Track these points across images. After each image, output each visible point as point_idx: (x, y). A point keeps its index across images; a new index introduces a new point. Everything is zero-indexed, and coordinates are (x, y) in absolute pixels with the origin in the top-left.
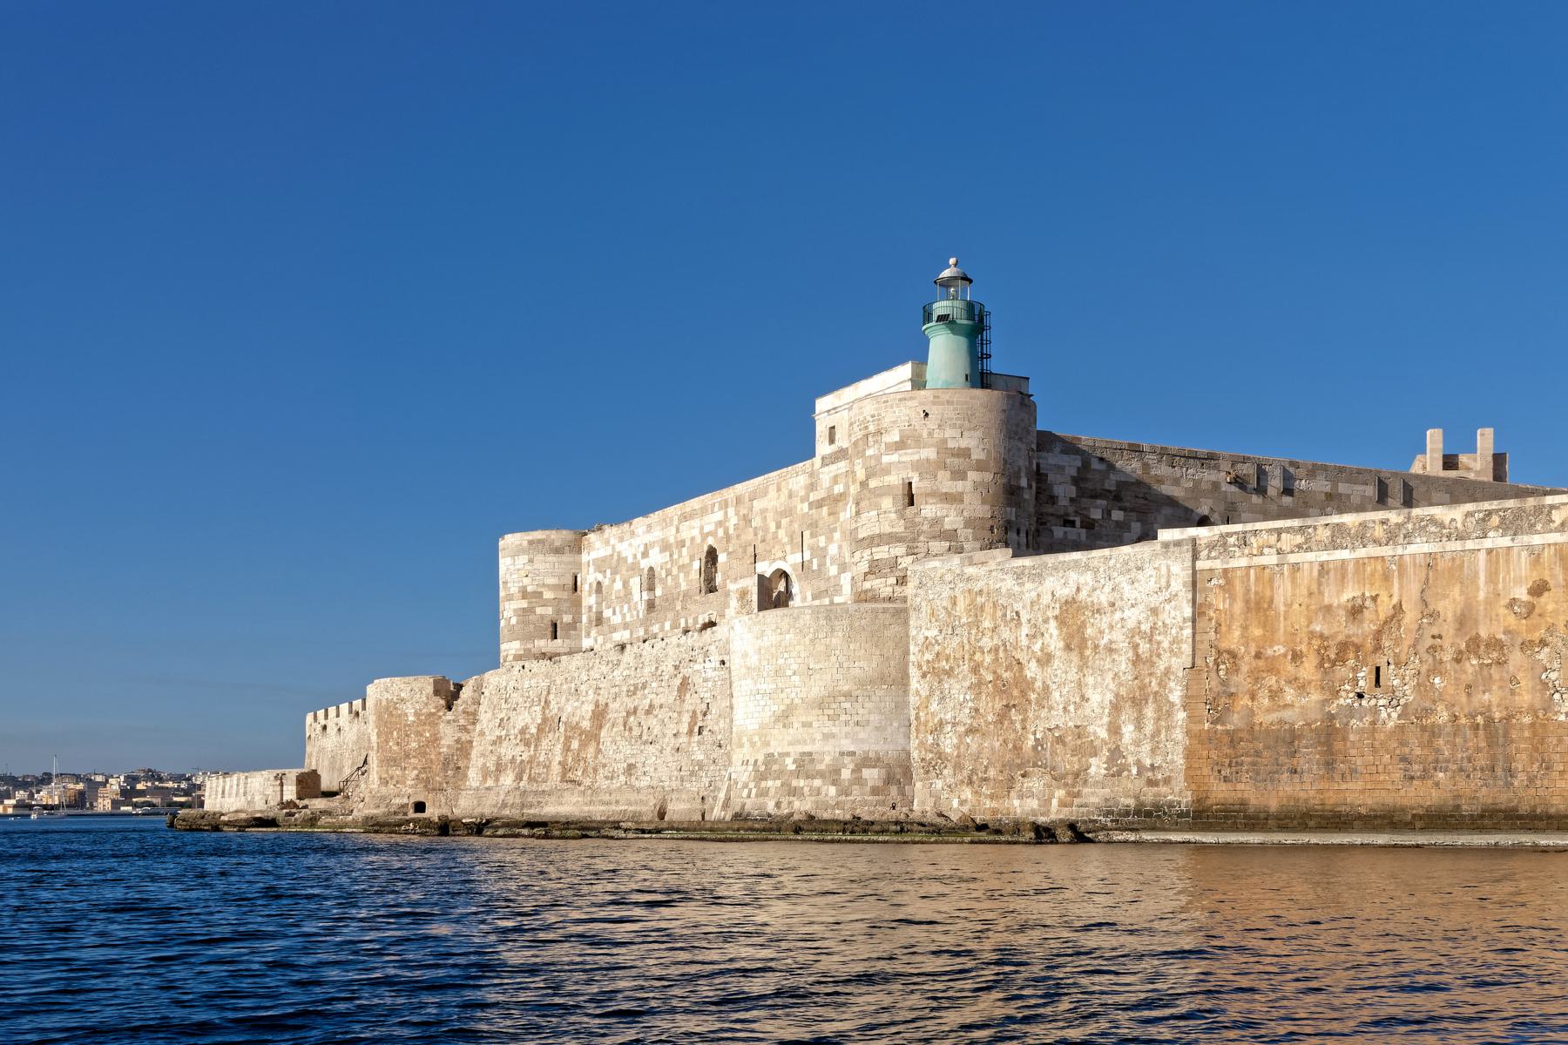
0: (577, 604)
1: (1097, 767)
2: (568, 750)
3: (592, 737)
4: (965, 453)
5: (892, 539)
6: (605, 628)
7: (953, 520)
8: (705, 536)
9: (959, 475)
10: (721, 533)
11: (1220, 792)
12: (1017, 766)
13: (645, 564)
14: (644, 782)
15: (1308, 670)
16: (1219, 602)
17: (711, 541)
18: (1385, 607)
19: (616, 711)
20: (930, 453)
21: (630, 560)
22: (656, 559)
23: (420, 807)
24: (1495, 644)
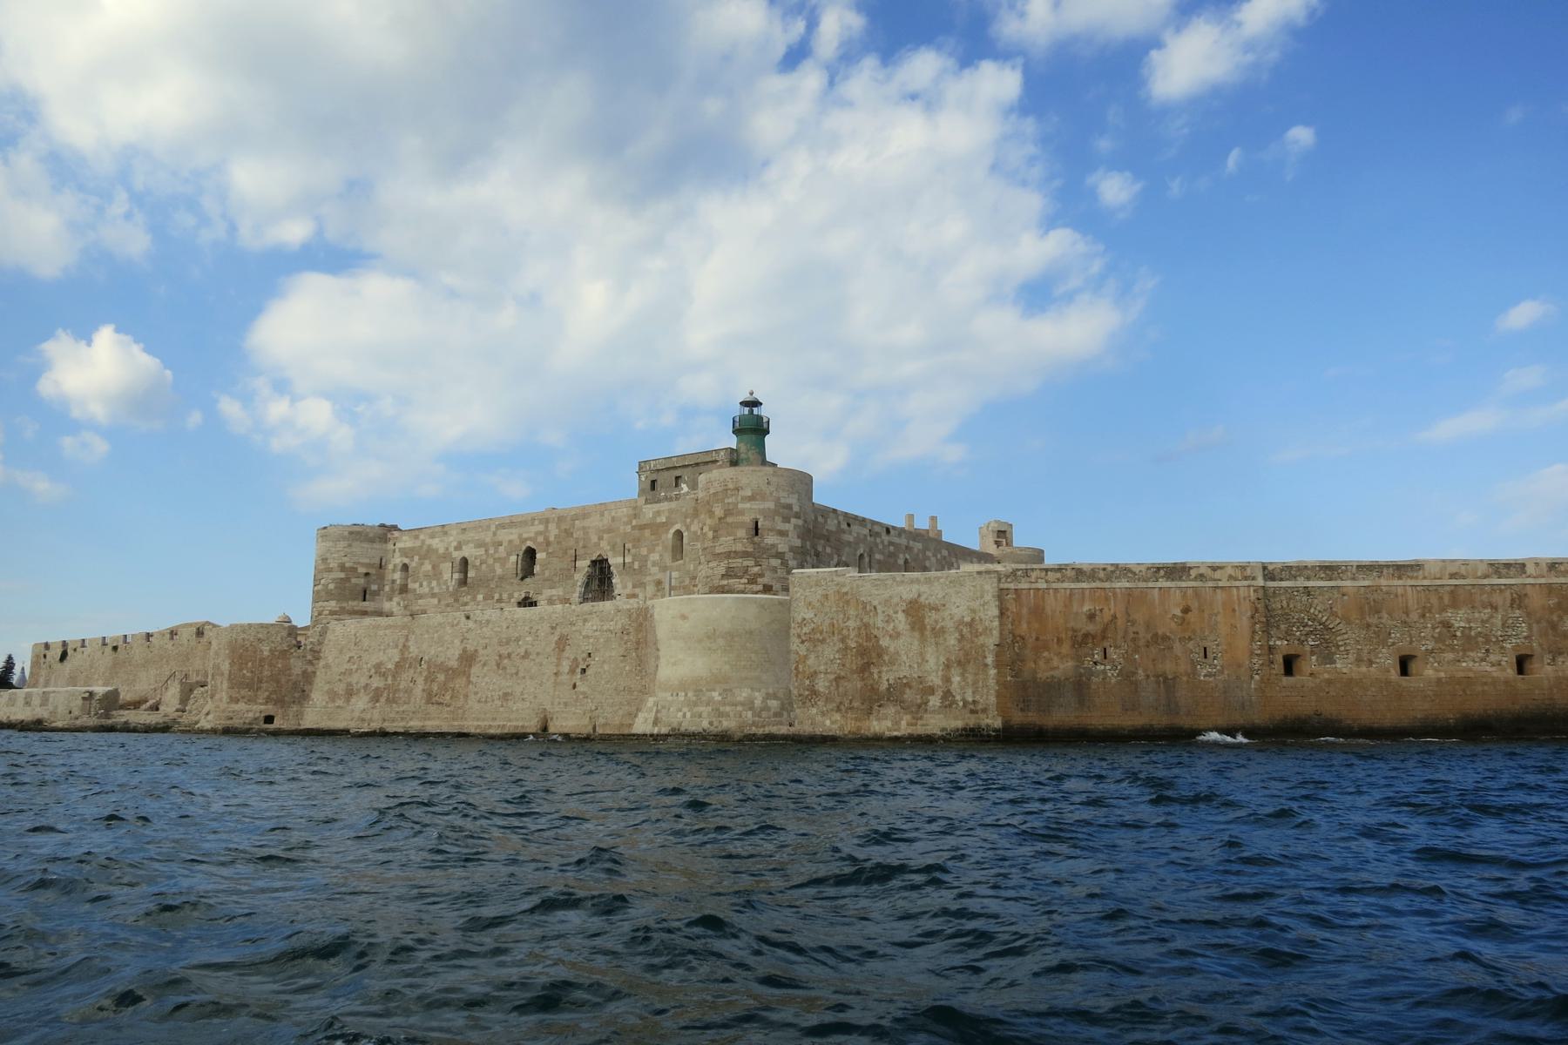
0: (381, 578)
1: (935, 701)
4: (789, 507)
5: (746, 555)
6: (410, 596)
7: (783, 547)
9: (786, 520)
11: (1018, 718)
12: (873, 699)
13: (457, 555)
15: (1066, 648)
16: (1013, 607)
17: (529, 544)
18: (1107, 616)
20: (771, 505)
21: (441, 551)
22: (467, 551)
23: (269, 719)
24: (1165, 638)
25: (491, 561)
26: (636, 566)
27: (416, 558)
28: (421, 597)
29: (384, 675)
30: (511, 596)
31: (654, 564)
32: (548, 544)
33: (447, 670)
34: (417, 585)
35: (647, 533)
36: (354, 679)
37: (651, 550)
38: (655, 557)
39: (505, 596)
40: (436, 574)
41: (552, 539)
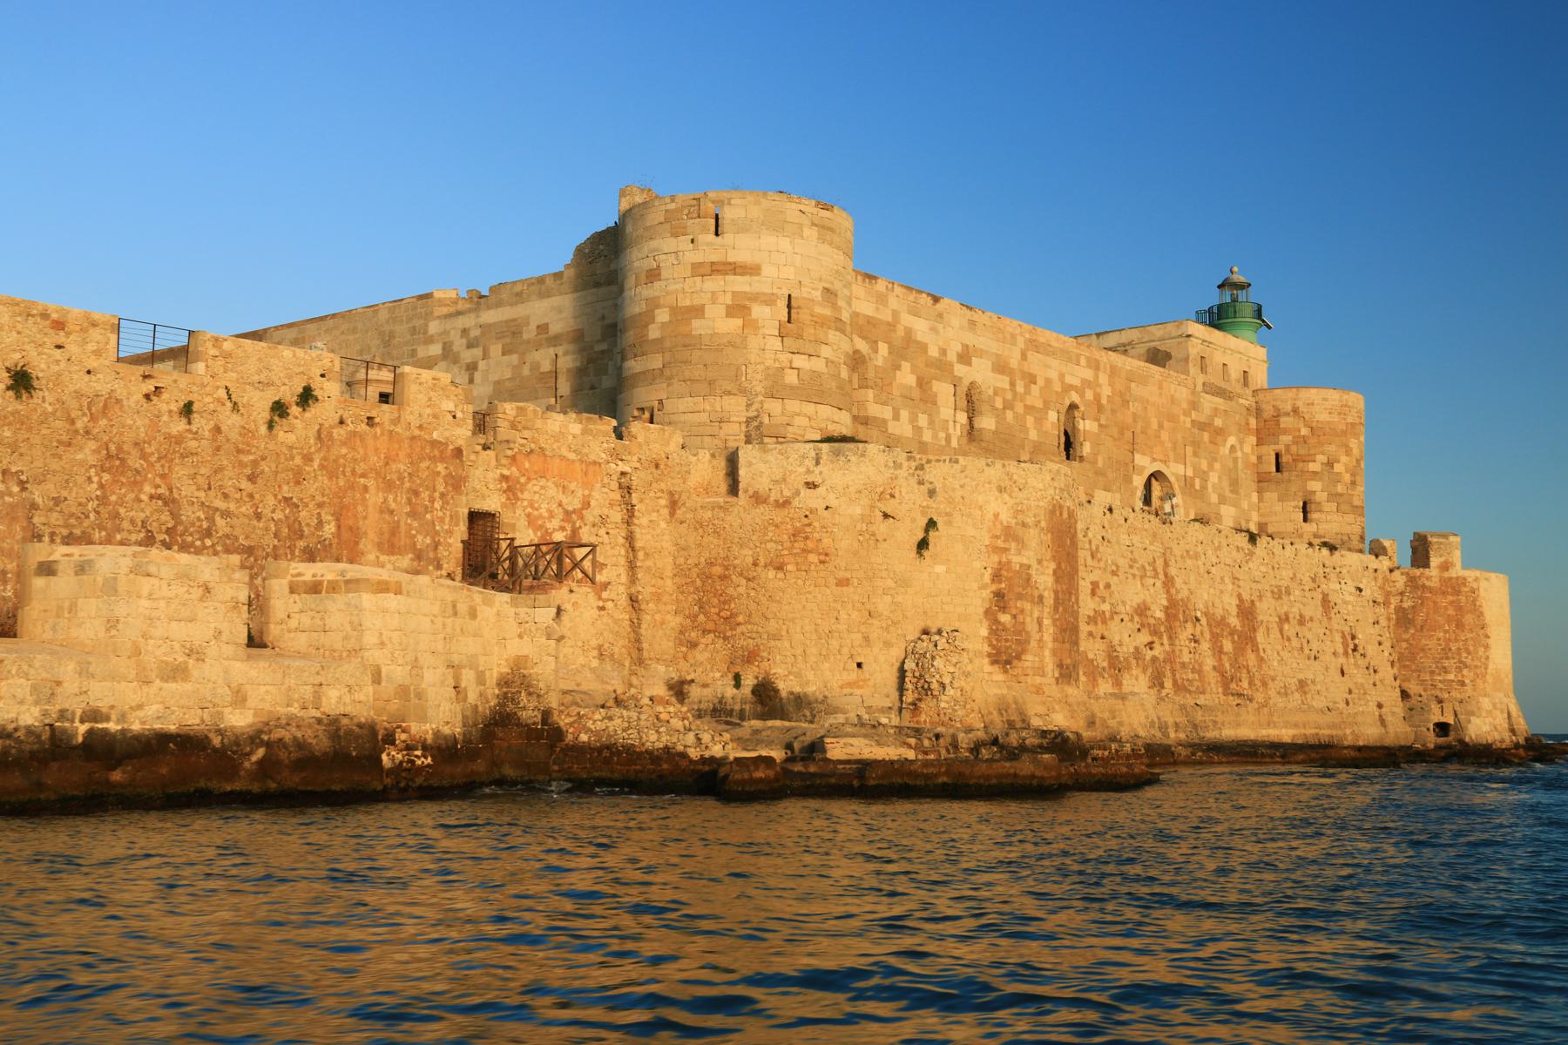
2: (1221, 652)
3: (1246, 638)
8: (1068, 388)
10: (1089, 395)
14: (1319, 703)
17: (1075, 398)
19: (1266, 610)
22: (980, 373)
25: (1020, 408)
32: (1100, 408)
40: (924, 398)
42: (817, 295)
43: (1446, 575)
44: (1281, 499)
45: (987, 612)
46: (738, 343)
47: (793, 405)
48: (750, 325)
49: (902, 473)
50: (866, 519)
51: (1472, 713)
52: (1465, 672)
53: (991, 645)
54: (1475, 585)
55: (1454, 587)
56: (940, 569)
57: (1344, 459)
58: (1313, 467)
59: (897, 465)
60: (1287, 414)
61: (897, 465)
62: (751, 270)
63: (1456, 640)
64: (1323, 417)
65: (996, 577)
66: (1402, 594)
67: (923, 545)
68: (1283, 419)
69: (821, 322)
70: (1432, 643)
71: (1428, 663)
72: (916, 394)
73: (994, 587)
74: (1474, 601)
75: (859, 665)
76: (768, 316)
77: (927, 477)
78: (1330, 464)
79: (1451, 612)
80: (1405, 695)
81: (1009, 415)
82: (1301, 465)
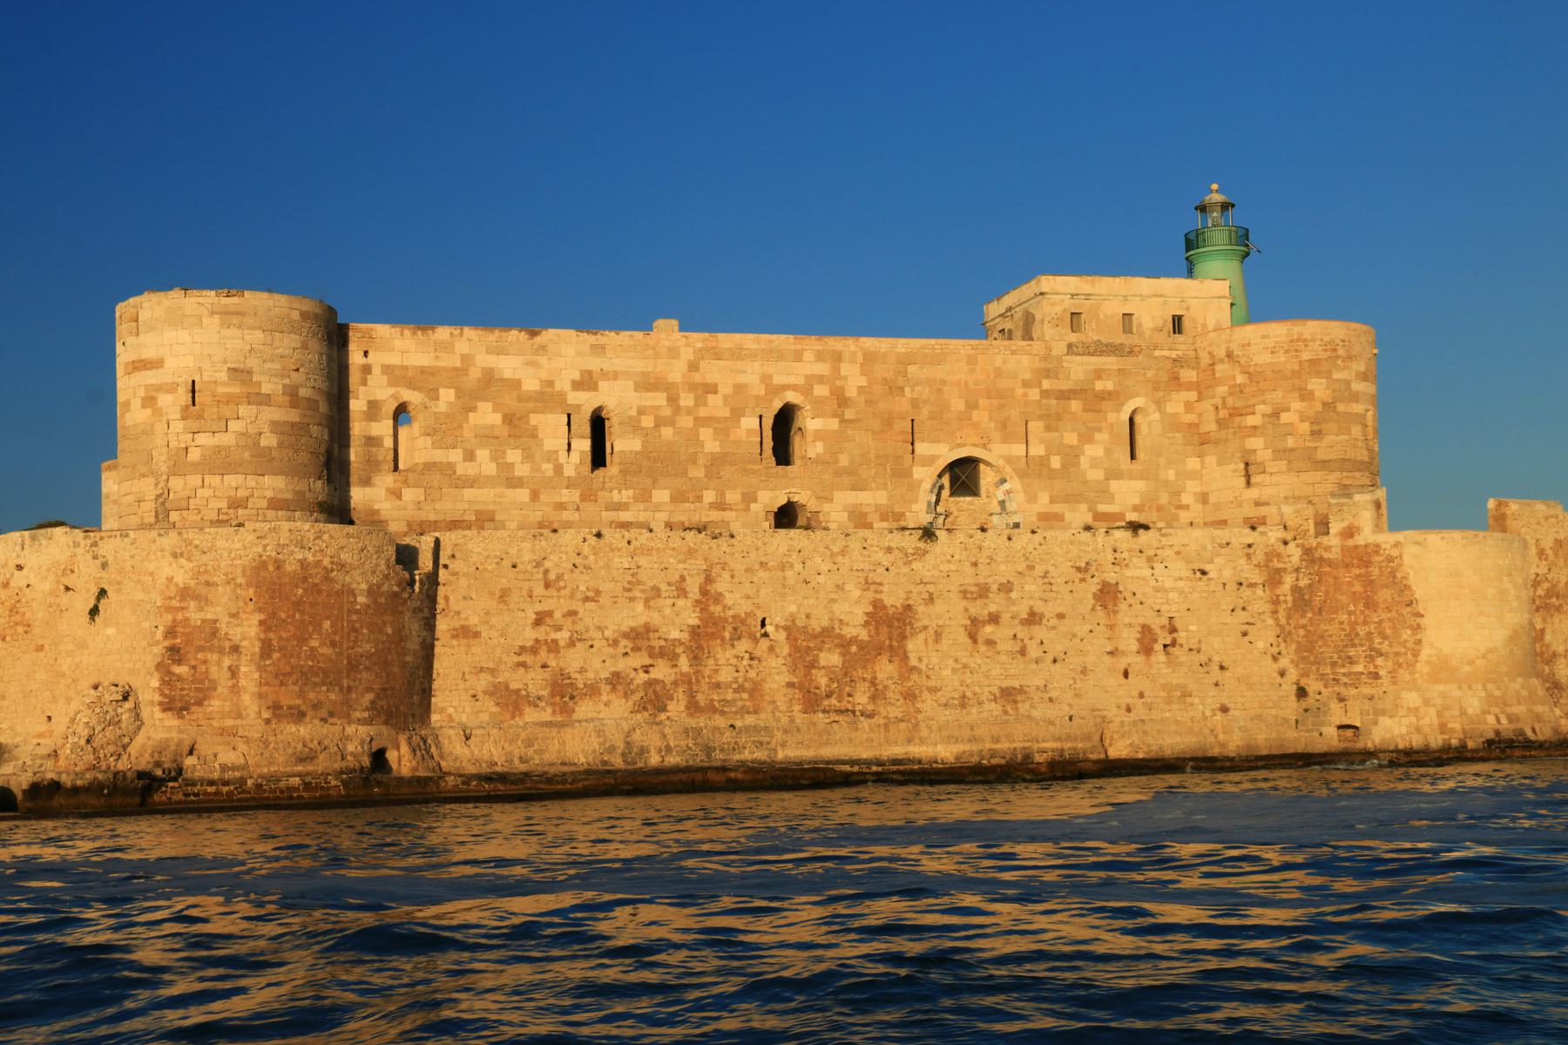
13: (586, 402)
17: (792, 397)
25: (686, 422)
26: (1056, 462)
27: (447, 395)
28: (471, 482)
29: (667, 653)
30: (749, 498)
31: (1094, 463)
32: (842, 401)
33: (844, 644)
34: (455, 456)
35: (1075, 405)
36: (572, 661)
37: (1087, 438)
38: (1093, 451)
39: (733, 497)
41: (852, 393)
42: (223, 376)
43: (1350, 543)
44: (1220, 463)
45: (158, 666)
46: (148, 432)
47: (195, 480)
48: (158, 412)
49: (80, 551)
50: (53, 593)
51: (1384, 712)
52: (1379, 661)
53: (163, 694)
54: (1394, 553)
55: (1363, 557)
56: (111, 631)
57: (1296, 405)
58: (1251, 420)
59: (76, 544)
60: (1221, 361)
61: (76, 544)
62: (156, 364)
63: (1365, 623)
64: (1266, 358)
65: (170, 632)
66: (1297, 570)
67: (94, 612)
68: (1218, 367)
69: (231, 400)
70: (1332, 628)
71: (1329, 653)
72: (504, 431)
73: (167, 643)
74: (1393, 574)
75: (49, 718)
76: (172, 403)
77: (101, 552)
78: (1276, 414)
79: (1358, 588)
80: (1302, 693)
81: (667, 432)
82: (1238, 419)
